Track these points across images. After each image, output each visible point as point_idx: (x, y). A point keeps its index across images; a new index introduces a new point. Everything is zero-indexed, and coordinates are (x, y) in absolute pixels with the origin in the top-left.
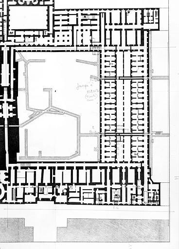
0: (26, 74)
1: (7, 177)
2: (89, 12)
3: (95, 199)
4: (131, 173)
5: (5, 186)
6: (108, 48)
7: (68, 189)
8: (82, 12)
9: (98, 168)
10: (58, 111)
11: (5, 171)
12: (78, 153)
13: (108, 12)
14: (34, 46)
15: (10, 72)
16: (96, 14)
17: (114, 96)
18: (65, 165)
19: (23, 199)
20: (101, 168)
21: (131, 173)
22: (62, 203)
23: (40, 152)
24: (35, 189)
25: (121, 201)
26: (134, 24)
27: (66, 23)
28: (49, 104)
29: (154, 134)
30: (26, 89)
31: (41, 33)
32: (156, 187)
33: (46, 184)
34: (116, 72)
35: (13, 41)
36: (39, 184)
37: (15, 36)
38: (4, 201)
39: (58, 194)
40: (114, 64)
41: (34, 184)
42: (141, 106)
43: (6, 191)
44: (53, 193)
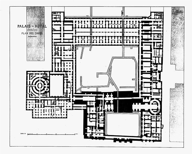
0: (89, 87)
1: (147, 98)
2: (54, 52)
3: (159, 49)
4: (145, 28)
5: (152, 99)
6: (74, 41)
7: (154, 64)
8: (54, 55)
9: (142, 47)
10: (110, 69)
11: (144, 99)
12: (133, 58)
13: (54, 41)
14: (73, 82)
15: (87, 96)
16: (55, 47)
17: (101, 38)
18: (140, 65)
19: (159, 89)
20: (142, 45)
21: (145, 28)
22: (162, 67)
23: (133, 79)
24: (154, 83)
25: (161, 34)
26: (60, 26)
27: (60, 64)
28: (106, 74)
29: (123, 15)
30: (97, 87)
31: (65, 78)
32: (153, 14)
33: (151, 76)
34: (87, 37)
35: (70, 94)
36: (151, 80)
37: (67, 93)
38: (160, 100)
39: (157, 70)
40: (83, 37)
41: (151, 83)
42: (107, 23)
43: (155, 99)
44: (156, 72)
